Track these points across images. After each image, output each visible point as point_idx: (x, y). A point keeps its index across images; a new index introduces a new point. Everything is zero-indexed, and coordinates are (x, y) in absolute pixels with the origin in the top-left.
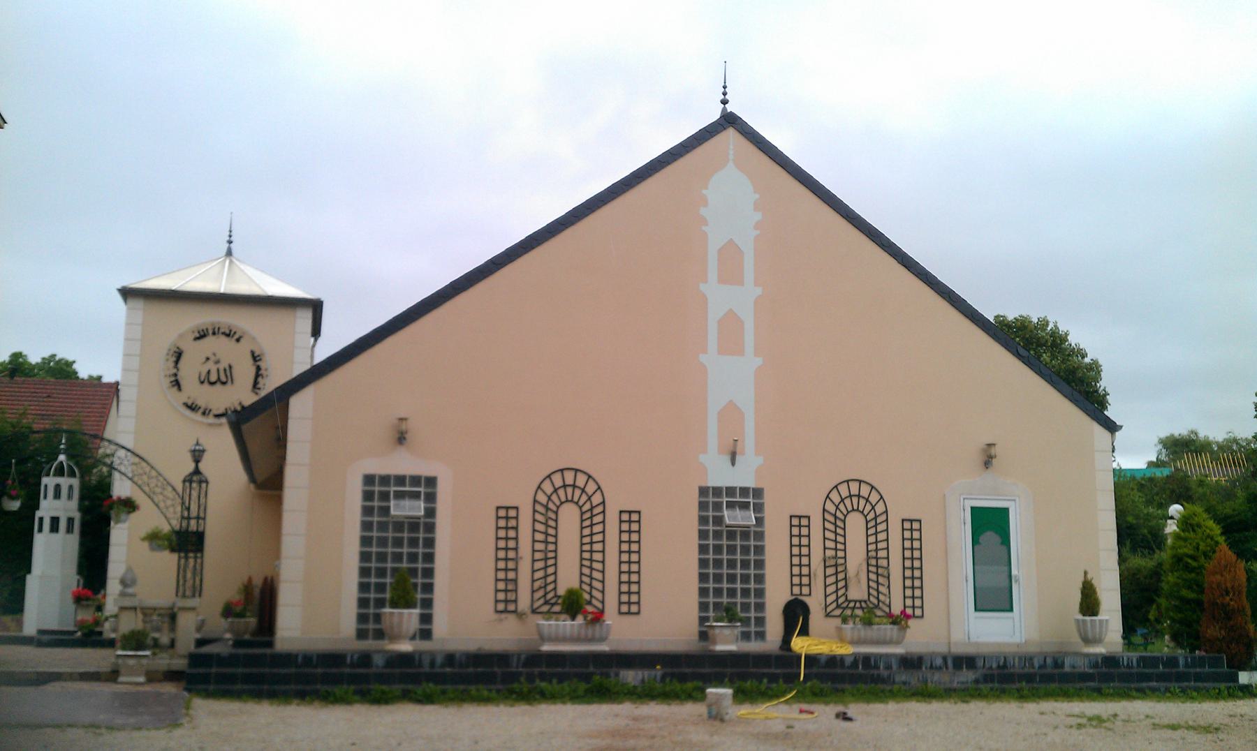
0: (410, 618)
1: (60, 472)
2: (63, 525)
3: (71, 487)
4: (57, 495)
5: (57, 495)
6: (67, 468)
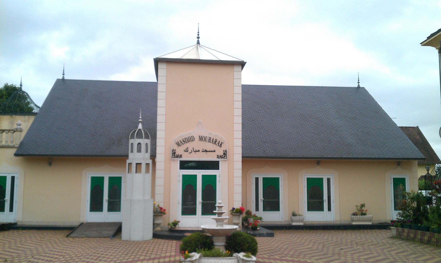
0: (409, 237)
1: (139, 136)
2: (143, 167)
3: (147, 144)
4: (139, 151)
5: (139, 151)
6: (145, 134)
